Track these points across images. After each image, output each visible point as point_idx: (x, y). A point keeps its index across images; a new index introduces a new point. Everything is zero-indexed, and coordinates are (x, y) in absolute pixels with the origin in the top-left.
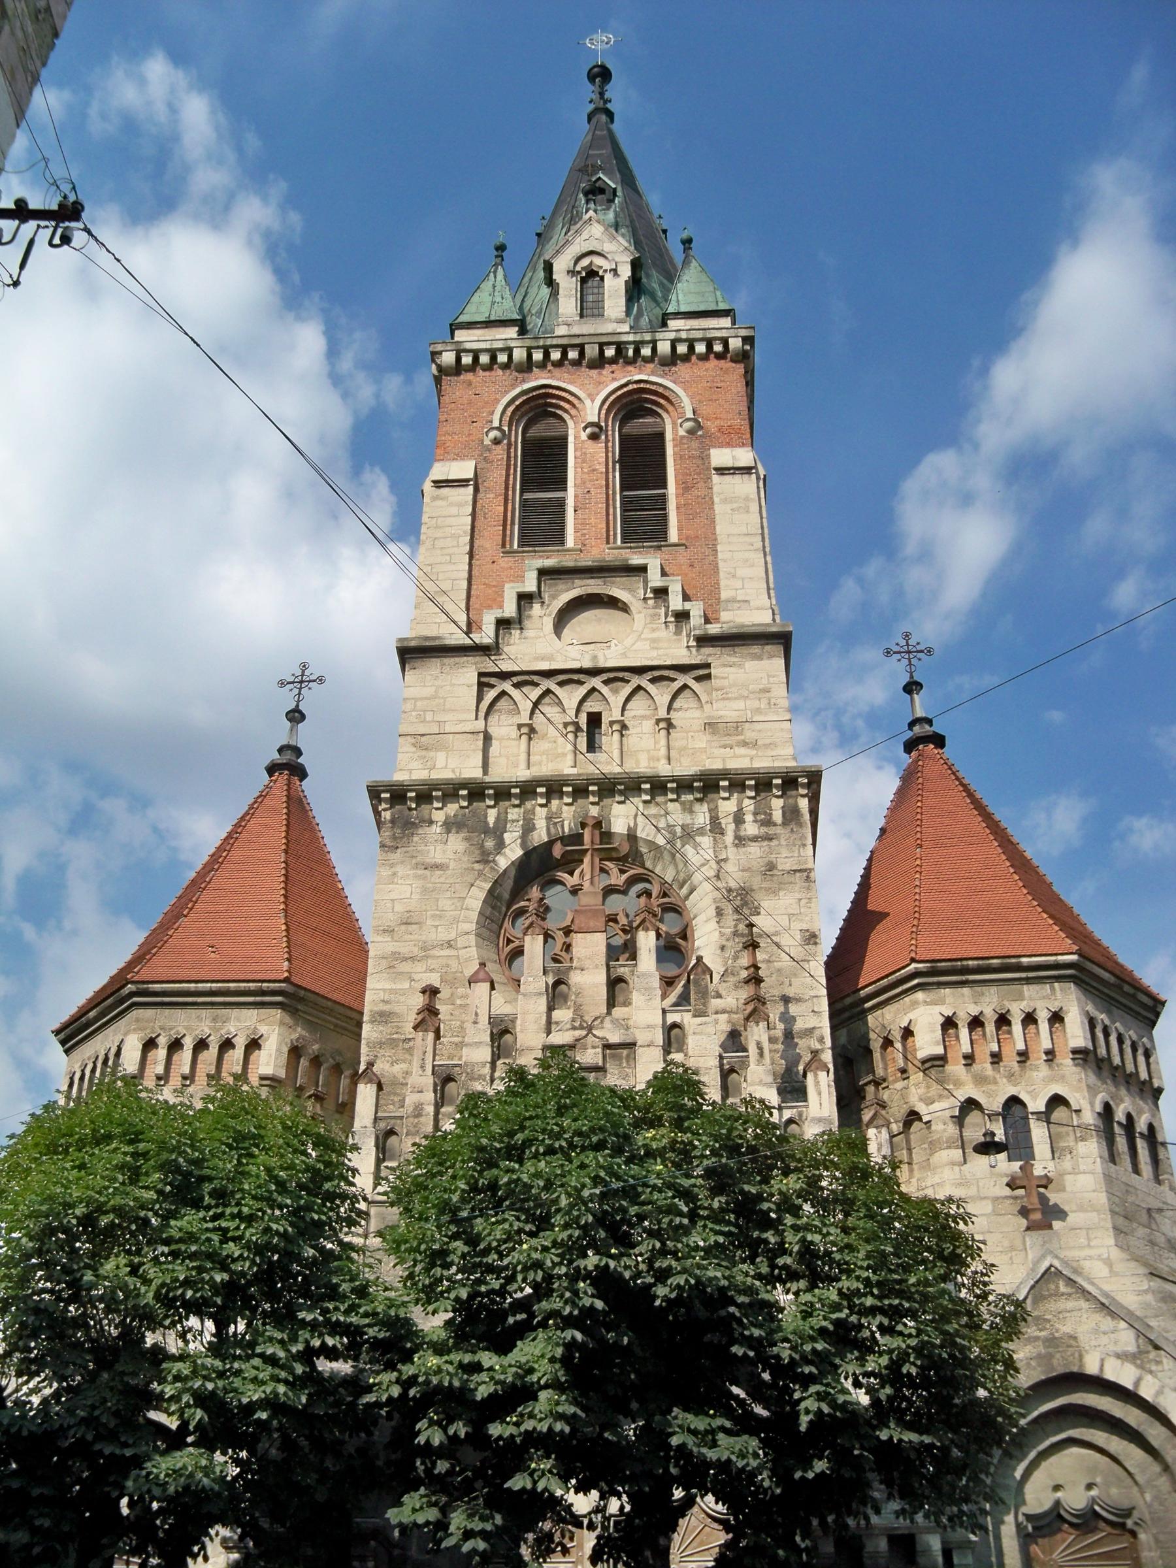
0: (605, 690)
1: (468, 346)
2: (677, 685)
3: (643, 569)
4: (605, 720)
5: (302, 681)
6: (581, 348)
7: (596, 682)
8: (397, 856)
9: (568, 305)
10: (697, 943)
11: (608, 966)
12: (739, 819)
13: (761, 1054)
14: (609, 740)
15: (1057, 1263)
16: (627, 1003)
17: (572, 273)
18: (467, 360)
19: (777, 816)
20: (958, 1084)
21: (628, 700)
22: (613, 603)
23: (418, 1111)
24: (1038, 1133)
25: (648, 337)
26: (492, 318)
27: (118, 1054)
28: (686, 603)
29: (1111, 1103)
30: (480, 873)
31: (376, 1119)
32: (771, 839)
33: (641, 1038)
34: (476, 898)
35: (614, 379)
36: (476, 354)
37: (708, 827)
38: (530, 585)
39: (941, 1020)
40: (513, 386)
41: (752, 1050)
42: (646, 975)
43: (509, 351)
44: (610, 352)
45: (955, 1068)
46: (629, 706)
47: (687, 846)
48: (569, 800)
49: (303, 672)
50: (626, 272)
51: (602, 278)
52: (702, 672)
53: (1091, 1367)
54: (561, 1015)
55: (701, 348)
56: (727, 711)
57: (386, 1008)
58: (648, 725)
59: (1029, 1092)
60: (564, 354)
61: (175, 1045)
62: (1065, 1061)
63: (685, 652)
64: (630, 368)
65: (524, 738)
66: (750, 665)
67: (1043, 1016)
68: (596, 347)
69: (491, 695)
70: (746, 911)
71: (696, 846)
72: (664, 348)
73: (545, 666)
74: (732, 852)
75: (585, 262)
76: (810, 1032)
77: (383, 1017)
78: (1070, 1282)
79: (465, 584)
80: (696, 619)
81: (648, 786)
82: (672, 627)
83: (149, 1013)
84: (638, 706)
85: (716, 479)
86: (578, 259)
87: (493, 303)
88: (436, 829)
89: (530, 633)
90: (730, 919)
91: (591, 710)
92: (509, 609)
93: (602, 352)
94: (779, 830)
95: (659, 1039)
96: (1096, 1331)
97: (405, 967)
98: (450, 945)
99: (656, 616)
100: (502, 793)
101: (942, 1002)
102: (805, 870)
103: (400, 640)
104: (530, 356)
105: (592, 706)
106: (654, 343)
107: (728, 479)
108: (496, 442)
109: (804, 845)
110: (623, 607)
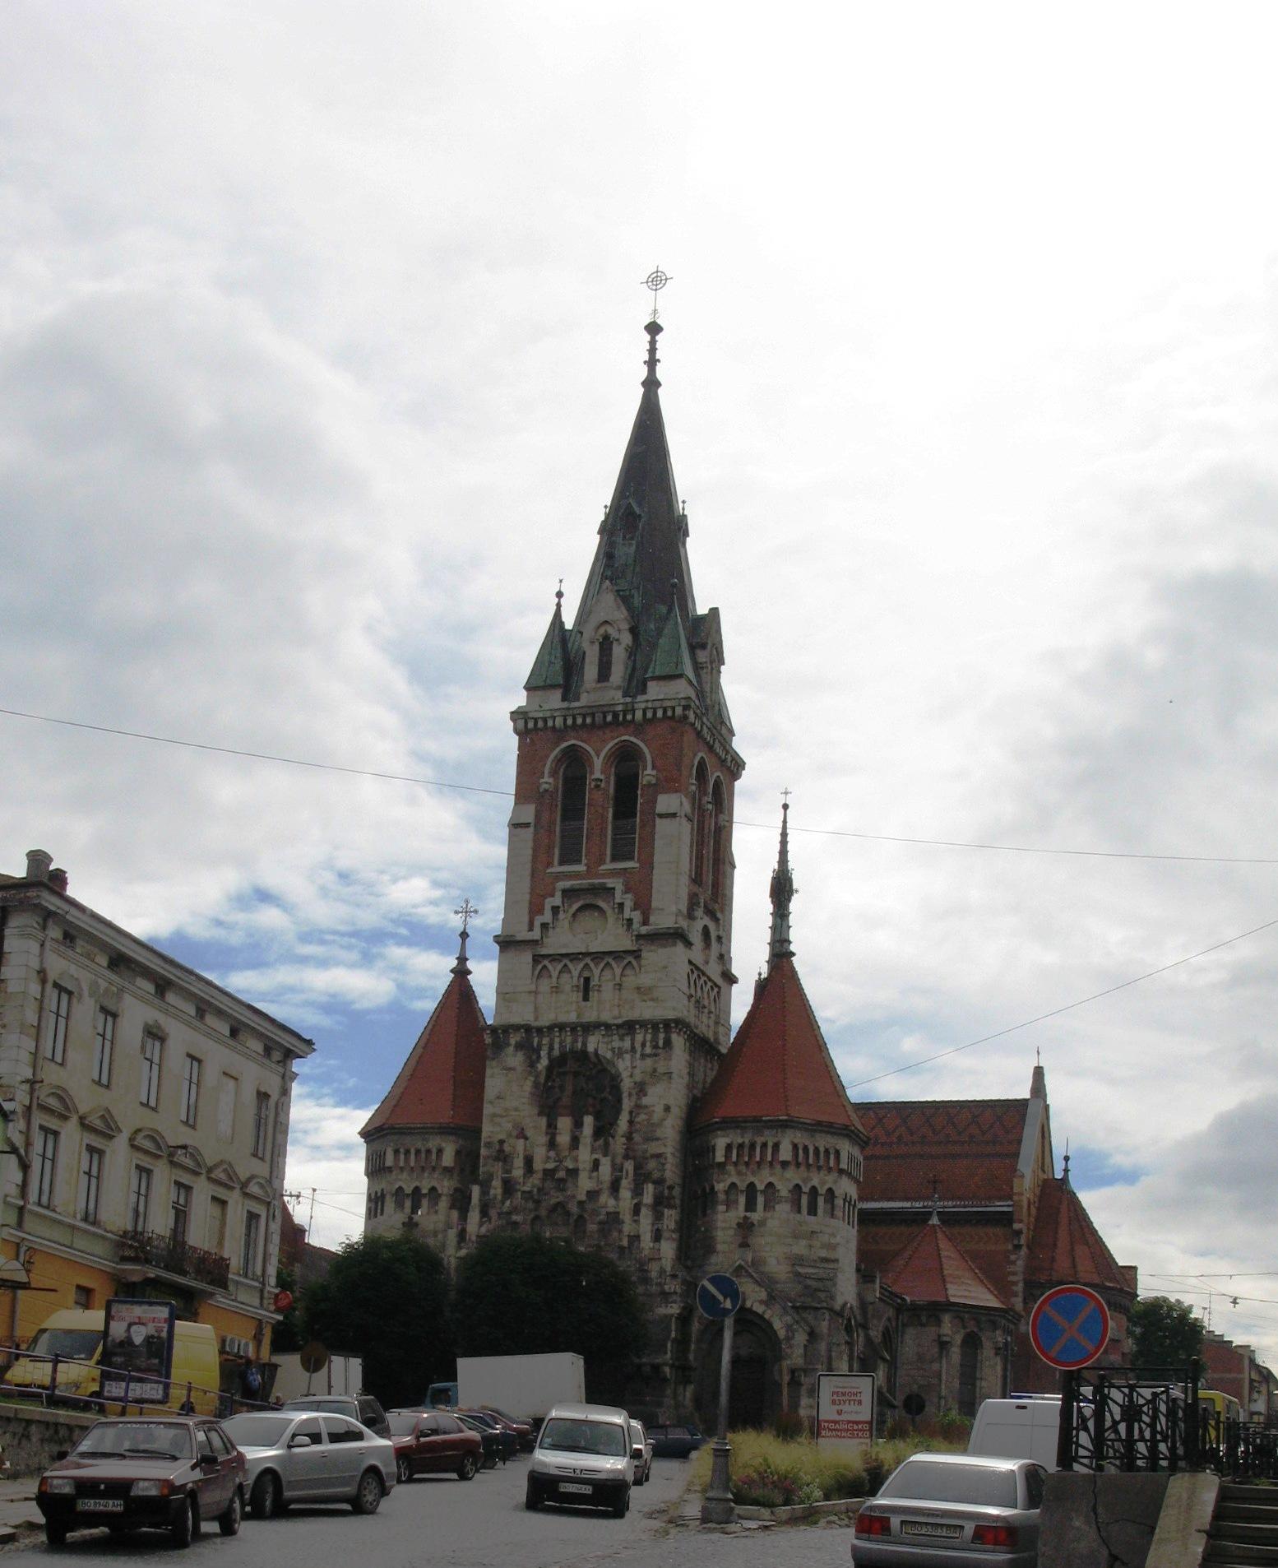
0: (592, 965)
1: (531, 715)
2: (626, 962)
4: (592, 984)
6: (593, 715)
7: (588, 960)
8: (494, 1063)
9: (591, 671)
10: (623, 1107)
11: (571, 1131)
12: (643, 1045)
13: (627, 1175)
14: (593, 995)
15: (743, 1263)
16: (577, 1148)
17: (592, 643)
18: (531, 725)
19: (661, 1043)
20: (730, 1175)
21: (602, 970)
22: (598, 906)
23: (495, 1195)
24: (760, 1200)
25: (630, 707)
26: (548, 682)
27: (385, 1154)
28: (633, 913)
29: (801, 1183)
30: (530, 1073)
31: (480, 1200)
32: (656, 1056)
33: (581, 1166)
34: (528, 1085)
35: (613, 738)
36: (536, 720)
37: (629, 1048)
39: (725, 1145)
40: (557, 744)
41: (624, 1173)
42: (585, 1137)
43: (555, 717)
44: (609, 718)
45: (730, 1168)
46: (603, 973)
47: (620, 1060)
48: (569, 1034)
49: (467, 905)
50: (627, 639)
51: (612, 642)
52: (636, 954)
53: (748, 1304)
54: (552, 1154)
55: (660, 714)
56: (645, 979)
57: (488, 1140)
58: (611, 984)
59: (759, 1180)
60: (584, 720)
61: (407, 1152)
62: (778, 1167)
63: (629, 942)
64: (621, 727)
65: (554, 994)
66: (661, 951)
67: (770, 1144)
68: (601, 715)
69: (540, 967)
70: (641, 1094)
71: (623, 1060)
72: (639, 715)
73: (564, 951)
74: (639, 1062)
75: (602, 631)
76: (659, 1156)
77: (489, 1145)
78: (747, 1271)
79: (527, 897)
80: (635, 926)
81: (603, 1028)
82: (625, 927)
83: (396, 1137)
84: (607, 972)
85: (658, 820)
86: (598, 627)
87: (550, 663)
88: (511, 1049)
89: (558, 930)
90: (634, 1098)
91: (585, 976)
92: (547, 917)
93: (605, 717)
94: (660, 1051)
95: (588, 1169)
96: (752, 1291)
97: (498, 1120)
98: (516, 1109)
99: (618, 919)
100: (539, 1030)
101: (728, 1136)
102: (668, 1073)
103: (495, 937)
104: (565, 720)
105: (586, 974)
106: (633, 711)
107: (664, 820)
108: (546, 791)
109: (670, 1059)
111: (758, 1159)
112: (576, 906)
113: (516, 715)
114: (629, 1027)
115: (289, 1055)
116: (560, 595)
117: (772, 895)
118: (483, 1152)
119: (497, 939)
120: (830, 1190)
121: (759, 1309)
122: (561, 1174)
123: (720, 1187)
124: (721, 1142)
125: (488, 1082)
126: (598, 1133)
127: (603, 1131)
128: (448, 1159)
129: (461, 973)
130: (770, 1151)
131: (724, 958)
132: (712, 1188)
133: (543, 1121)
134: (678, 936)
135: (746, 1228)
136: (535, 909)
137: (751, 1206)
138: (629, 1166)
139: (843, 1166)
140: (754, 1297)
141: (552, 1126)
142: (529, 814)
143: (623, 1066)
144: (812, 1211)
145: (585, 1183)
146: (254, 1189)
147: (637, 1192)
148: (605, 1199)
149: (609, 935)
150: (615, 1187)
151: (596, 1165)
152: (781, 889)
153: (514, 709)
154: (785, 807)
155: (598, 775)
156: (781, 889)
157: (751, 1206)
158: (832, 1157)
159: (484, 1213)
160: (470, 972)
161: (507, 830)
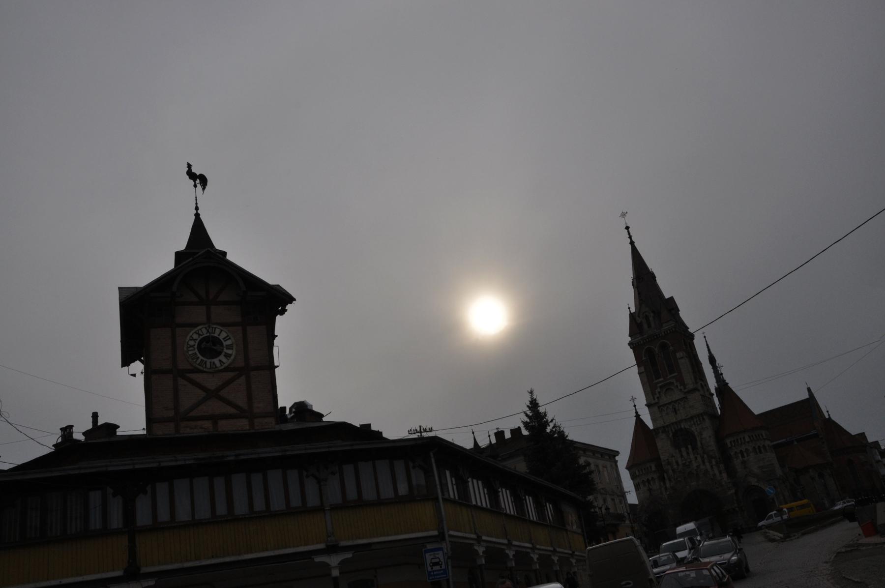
3: (673, 383)
5: (633, 399)
9: (645, 326)
18: (634, 345)
19: (701, 420)
24: (745, 454)
36: (635, 344)
38: (659, 390)
50: (652, 315)
52: (686, 398)
54: (683, 459)
55: (669, 332)
61: (642, 470)
72: (663, 334)
73: (665, 403)
80: (683, 390)
92: (658, 395)
100: (667, 426)
106: (661, 333)
110: (672, 389)
111: (740, 443)
112: (665, 390)
113: (629, 344)
114: (692, 418)
115: (614, 456)
116: (629, 308)
117: (710, 363)
118: (663, 464)
119: (646, 405)
120: (764, 446)
121: (757, 484)
122: (687, 463)
123: (732, 454)
124: (728, 441)
125: (658, 444)
126: (693, 449)
127: (694, 448)
128: (654, 468)
129: (638, 416)
130: (742, 439)
131: (709, 390)
132: (730, 455)
133: (677, 451)
134: (695, 390)
135: (744, 462)
136: (653, 394)
137: (743, 456)
138: (705, 456)
139: (765, 437)
140: (753, 481)
141: (680, 451)
142: (643, 369)
143: (693, 429)
144: (761, 452)
145: (695, 465)
146: (619, 494)
147: (710, 462)
148: (702, 467)
149: (677, 395)
150: (704, 462)
151: (696, 458)
152: (712, 360)
153: (628, 342)
154: (705, 337)
155: (657, 352)
156: (712, 360)
157: (743, 456)
158: (761, 436)
159: (670, 480)
160: (640, 415)
161: (638, 375)
